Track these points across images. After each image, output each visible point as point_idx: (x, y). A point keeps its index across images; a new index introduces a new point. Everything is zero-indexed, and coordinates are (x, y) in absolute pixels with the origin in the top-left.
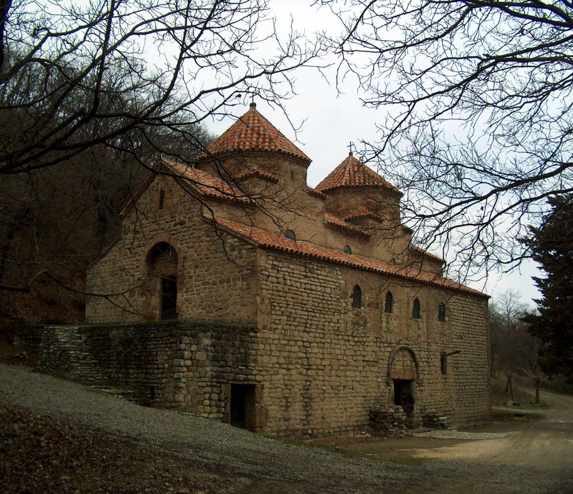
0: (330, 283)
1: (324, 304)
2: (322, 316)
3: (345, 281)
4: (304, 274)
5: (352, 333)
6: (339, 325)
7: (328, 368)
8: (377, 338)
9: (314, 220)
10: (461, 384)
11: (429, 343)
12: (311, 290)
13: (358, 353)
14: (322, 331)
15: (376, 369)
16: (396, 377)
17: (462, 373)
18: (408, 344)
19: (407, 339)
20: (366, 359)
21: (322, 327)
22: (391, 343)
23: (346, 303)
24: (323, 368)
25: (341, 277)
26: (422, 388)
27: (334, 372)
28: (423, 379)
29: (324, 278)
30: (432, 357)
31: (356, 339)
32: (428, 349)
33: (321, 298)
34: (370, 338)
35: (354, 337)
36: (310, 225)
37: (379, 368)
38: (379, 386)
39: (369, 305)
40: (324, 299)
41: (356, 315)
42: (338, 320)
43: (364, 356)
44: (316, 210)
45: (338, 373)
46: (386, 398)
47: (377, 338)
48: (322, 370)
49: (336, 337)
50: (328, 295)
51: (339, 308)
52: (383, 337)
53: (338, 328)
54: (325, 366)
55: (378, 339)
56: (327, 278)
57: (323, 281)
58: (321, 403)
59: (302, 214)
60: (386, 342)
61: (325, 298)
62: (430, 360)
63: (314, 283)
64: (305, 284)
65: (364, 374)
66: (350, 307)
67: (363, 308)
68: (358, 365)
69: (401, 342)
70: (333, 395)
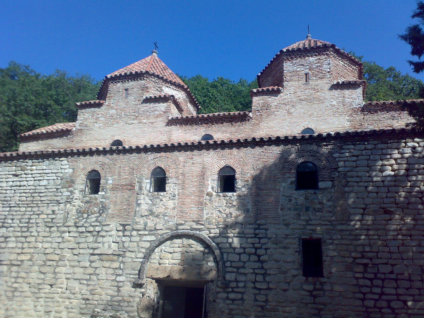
0: (48, 175)
1: (33, 197)
2: (30, 209)
3: (73, 169)
4: (14, 173)
5: (75, 223)
6: (54, 216)
7: (27, 264)
8: (124, 226)
9: (152, 123)
10: (384, 297)
11: (259, 225)
12: (20, 186)
13: (82, 246)
14: (26, 225)
15: (116, 265)
16: (161, 275)
17: (393, 276)
18: (200, 230)
19: (197, 222)
20: (96, 252)
21: (27, 220)
22: (156, 229)
23: (71, 192)
24: (19, 263)
25: (68, 166)
26: (232, 296)
27: (36, 268)
28: (237, 281)
29: (40, 172)
30: (269, 245)
31: (83, 229)
32: (256, 235)
33: (31, 191)
34: (111, 226)
35: (78, 227)
36: (145, 129)
37: (122, 262)
38: (118, 287)
39: (113, 189)
40: (36, 193)
41: (87, 202)
42: (53, 211)
43: (94, 249)
44: (157, 113)
45: (44, 270)
46: (135, 305)
47: (124, 226)
48: (19, 265)
49: (48, 229)
50: (43, 188)
51: (58, 198)
52: (137, 223)
53: (52, 219)
54: (22, 261)
55: (127, 227)
56: (44, 171)
57: (39, 175)
58: (6, 302)
59: (135, 121)
60: (145, 229)
61: (37, 191)
62: (259, 252)
63: (24, 179)
64: (13, 182)
65: (91, 271)
66: (77, 194)
67: (103, 193)
68: (80, 260)
69: (181, 227)
70: (29, 294)
